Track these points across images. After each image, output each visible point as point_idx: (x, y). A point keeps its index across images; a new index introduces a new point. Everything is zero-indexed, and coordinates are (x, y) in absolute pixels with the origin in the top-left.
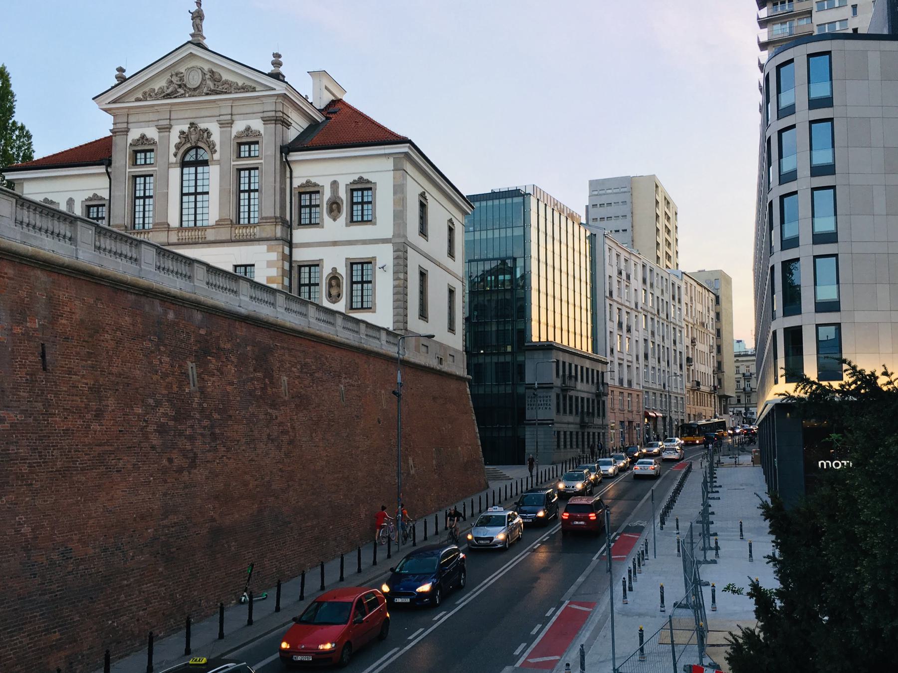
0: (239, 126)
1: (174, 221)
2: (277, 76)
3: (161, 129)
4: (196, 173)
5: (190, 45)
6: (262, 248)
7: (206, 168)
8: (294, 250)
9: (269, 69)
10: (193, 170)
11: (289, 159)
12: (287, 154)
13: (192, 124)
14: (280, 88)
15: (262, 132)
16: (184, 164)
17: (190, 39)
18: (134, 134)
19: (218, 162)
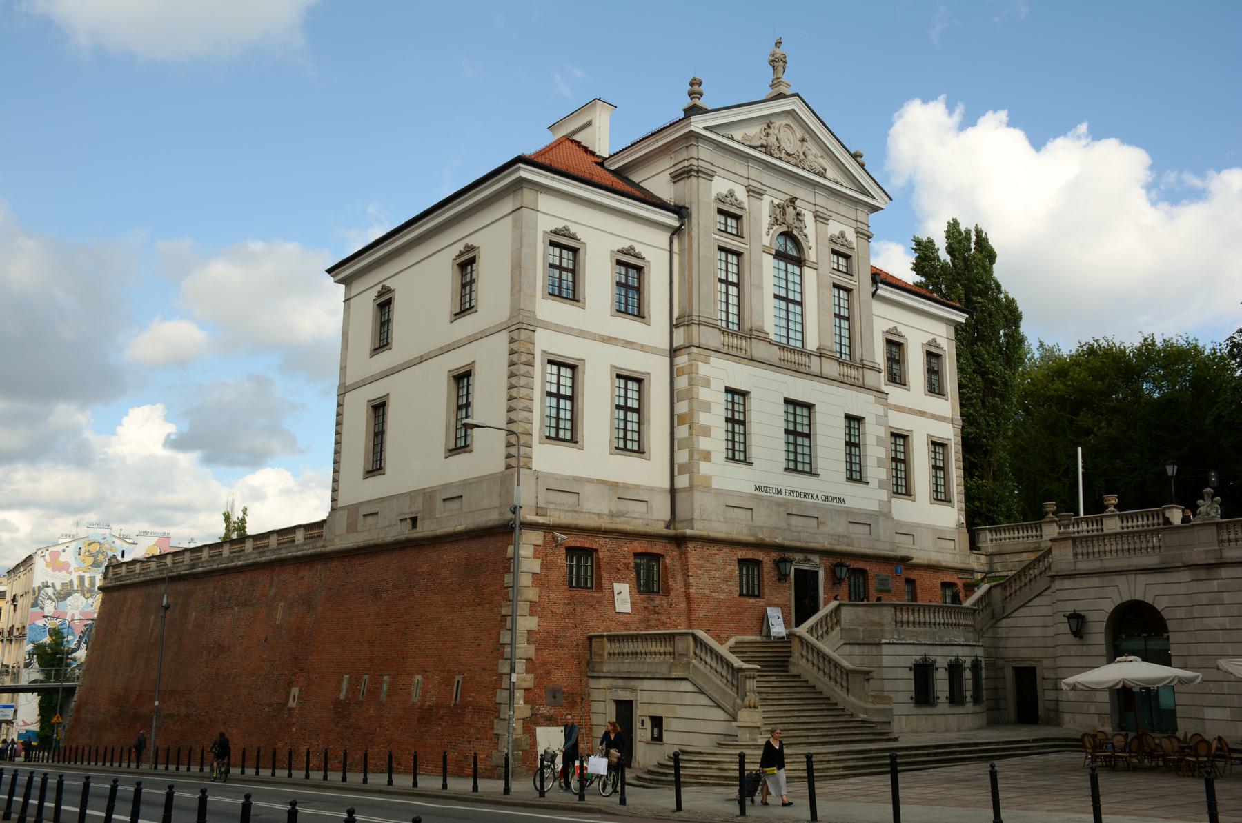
0: (834, 228)
3: (750, 191)
5: (796, 99)
7: (797, 270)
10: (782, 265)
13: (793, 201)
18: (720, 186)
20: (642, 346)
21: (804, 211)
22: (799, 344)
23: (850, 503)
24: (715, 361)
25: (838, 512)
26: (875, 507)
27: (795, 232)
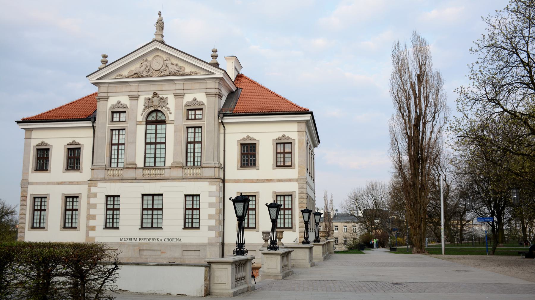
0: (189, 98)
1: (140, 164)
2: (216, 65)
3: (132, 98)
4: (156, 129)
5: (156, 43)
6: (206, 183)
7: (163, 126)
8: (226, 184)
9: (210, 60)
10: (154, 127)
11: (224, 121)
12: (222, 118)
13: (155, 94)
14: (219, 74)
15: (205, 102)
16: (148, 123)
17: (154, 37)
18: (113, 101)
19: (172, 122)
20: (78, 182)
21: (165, 96)
22: (162, 164)
23: (184, 241)
24: (100, 184)
25: (176, 246)
26: (206, 241)
27: (159, 109)
